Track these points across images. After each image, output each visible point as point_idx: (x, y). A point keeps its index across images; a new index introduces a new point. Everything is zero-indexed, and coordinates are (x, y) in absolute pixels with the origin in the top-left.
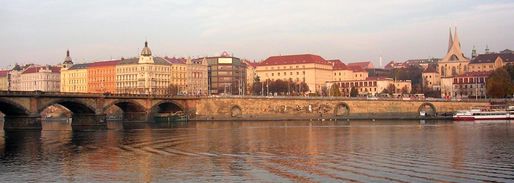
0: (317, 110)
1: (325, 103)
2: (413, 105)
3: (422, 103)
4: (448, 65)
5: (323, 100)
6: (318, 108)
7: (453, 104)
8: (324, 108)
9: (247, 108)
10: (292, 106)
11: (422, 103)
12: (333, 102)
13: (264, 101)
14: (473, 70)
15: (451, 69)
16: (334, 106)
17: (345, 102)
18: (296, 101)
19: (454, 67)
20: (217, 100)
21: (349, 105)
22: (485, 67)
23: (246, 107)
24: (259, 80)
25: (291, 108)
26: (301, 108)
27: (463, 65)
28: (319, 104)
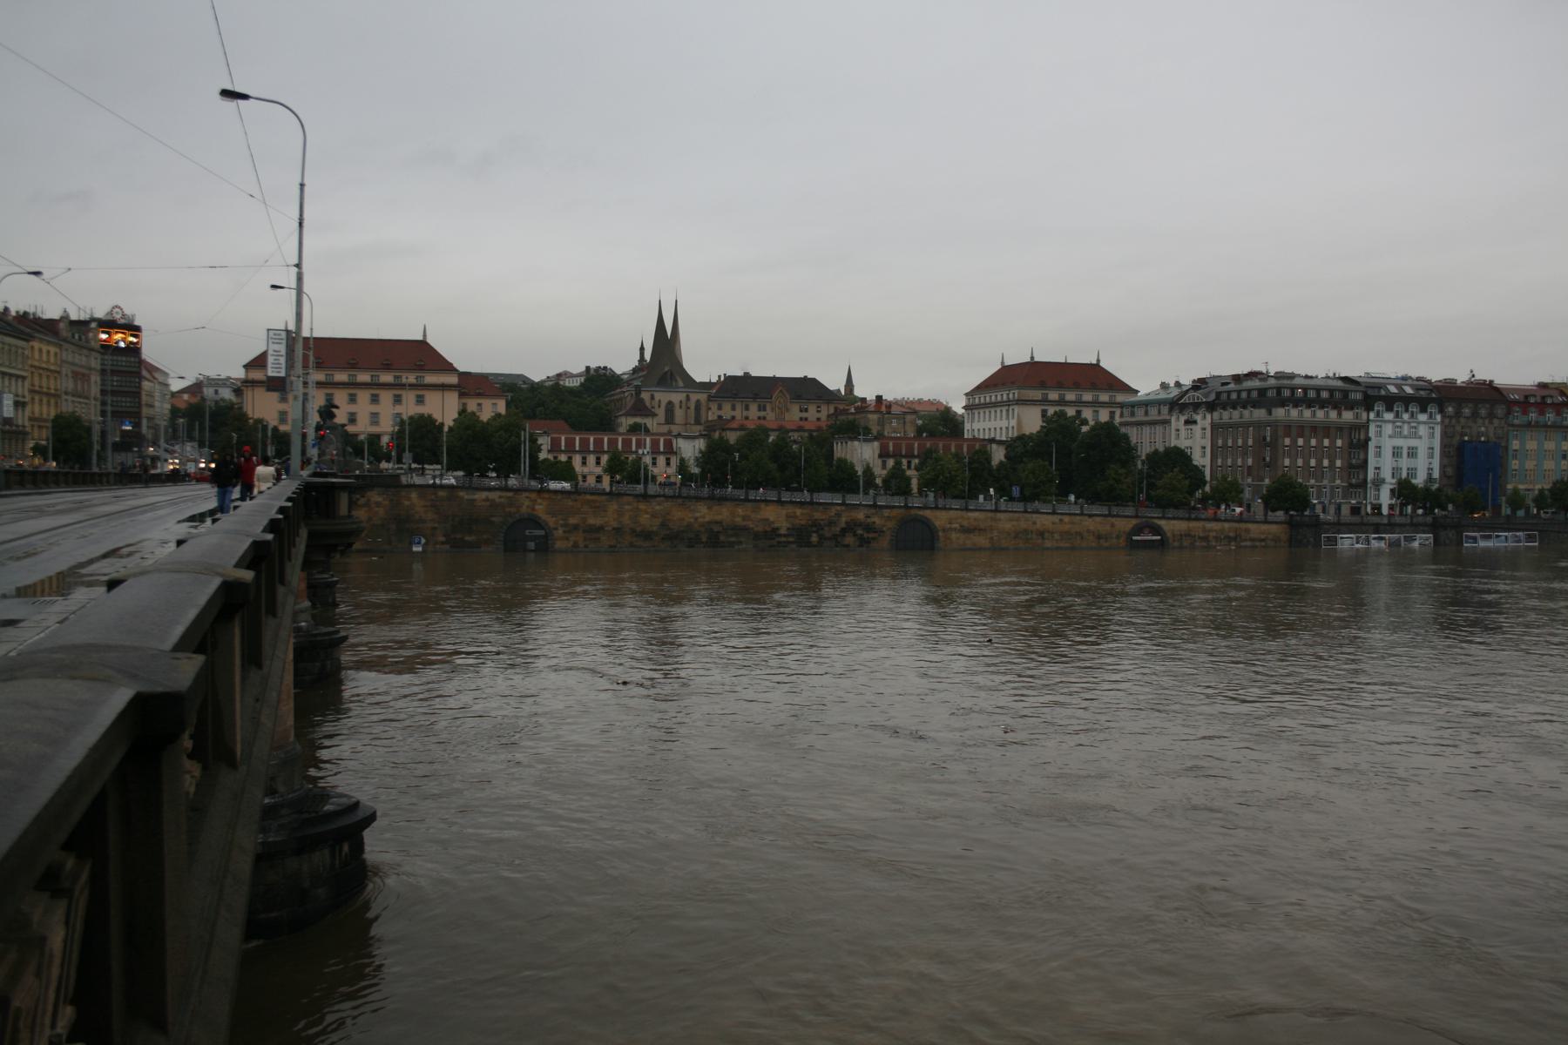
0: (835, 537)
2: (1113, 525)
3: (1134, 521)
4: (658, 396)
7: (1209, 525)
8: (860, 532)
9: (576, 527)
11: (1134, 521)
12: (886, 513)
13: (642, 506)
15: (663, 405)
16: (890, 524)
17: (927, 513)
18: (763, 505)
19: (670, 403)
20: (441, 493)
21: (937, 523)
22: (747, 408)
23: (572, 521)
24: (333, 416)
25: (745, 529)
26: (783, 531)
27: (694, 397)
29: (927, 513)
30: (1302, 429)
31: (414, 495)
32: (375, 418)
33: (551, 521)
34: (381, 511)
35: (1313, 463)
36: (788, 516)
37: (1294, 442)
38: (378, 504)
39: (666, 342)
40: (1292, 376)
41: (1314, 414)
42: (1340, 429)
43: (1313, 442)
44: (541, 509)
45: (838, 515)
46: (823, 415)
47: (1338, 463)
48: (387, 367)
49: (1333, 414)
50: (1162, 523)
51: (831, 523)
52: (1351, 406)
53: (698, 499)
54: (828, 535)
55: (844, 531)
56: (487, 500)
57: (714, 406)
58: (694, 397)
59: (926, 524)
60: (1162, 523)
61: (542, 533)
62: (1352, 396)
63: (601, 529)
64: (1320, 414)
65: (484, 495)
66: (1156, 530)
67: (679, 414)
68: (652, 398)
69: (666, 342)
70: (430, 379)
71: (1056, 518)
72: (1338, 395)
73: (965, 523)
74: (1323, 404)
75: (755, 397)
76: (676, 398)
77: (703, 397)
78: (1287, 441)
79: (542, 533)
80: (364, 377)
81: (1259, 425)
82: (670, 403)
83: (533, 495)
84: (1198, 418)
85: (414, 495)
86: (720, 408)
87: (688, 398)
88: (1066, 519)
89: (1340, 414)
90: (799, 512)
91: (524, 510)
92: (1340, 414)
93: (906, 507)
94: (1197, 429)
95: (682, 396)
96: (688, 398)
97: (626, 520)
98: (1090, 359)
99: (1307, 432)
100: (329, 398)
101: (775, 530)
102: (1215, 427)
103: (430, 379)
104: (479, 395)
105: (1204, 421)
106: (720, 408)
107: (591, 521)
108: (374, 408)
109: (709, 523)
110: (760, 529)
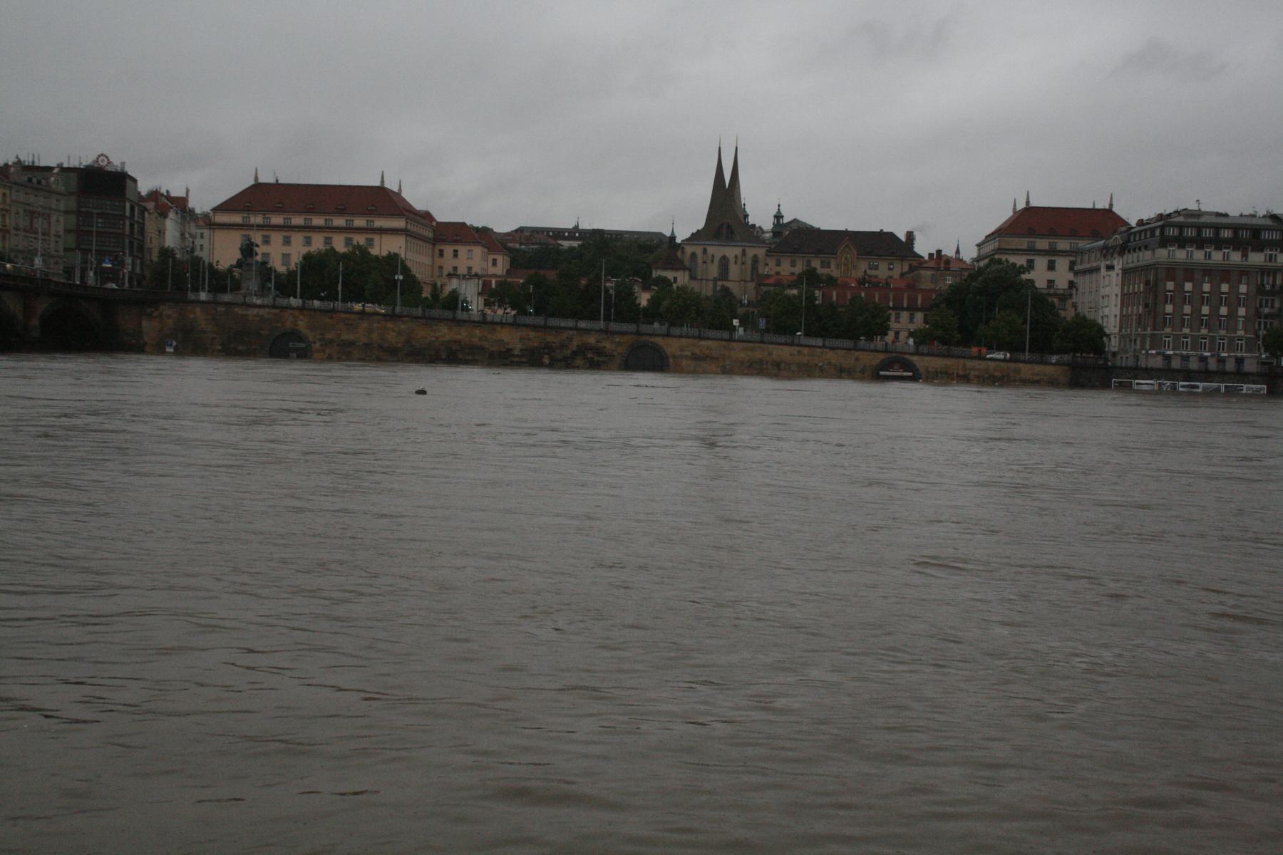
1: (592, 340)
3: (882, 356)
4: (710, 250)
5: (588, 331)
6: (568, 352)
7: (970, 363)
8: (590, 355)
9: (331, 341)
10: (486, 345)
11: (882, 356)
13: (390, 325)
14: (778, 269)
15: (716, 261)
17: (659, 340)
18: (498, 328)
19: (724, 258)
20: (221, 309)
21: (669, 351)
23: (330, 336)
25: (482, 348)
26: (516, 352)
27: (751, 252)
28: (575, 343)
29: (659, 340)
30: (1189, 272)
31: (198, 310)
32: (286, 257)
33: (310, 336)
34: (170, 322)
35: (1205, 310)
36: (521, 338)
37: (1180, 287)
38: (169, 317)
39: (725, 195)
40: (1198, 214)
41: (1226, 257)
42: (1244, 272)
43: (1206, 287)
44: (302, 324)
45: (570, 339)
46: (896, 273)
47: (1242, 311)
48: (341, 212)
49: (1236, 257)
50: (915, 359)
51: (563, 346)
52: (1259, 248)
53: (440, 320)
54: (560, 357)
55: (575, 354)
56: (257, 315)
57: (772, 262)
58: (751, 252)
59: (657, 349)
60: (915, 359)
61: (303, 345)
62: (1265, 235)
63: (351, 344)
64: (1217, 256)
65: (255, 311)
66: (907, 366)
67: (734, 270)
68: (705, 251)
69: (725, 195)
70: (380, 223)
71: (794, 349)
72: (1245, 234)
73: (697, 351)
74: (1219, 244)
75: (818, 252)
76: (732, 252)
77: (761, 252)
78: (1170, 285)
79: (303, 345)
80: (318, 221)
81: (1146, 268)
82: (724, 258)
83: (297, 313)
84: (1115, 262)
85: (198, 310)
86: (778, 264)
87: (744, 253)
88: (805, 351)
89: (1245, 256)
90: (532, 334)
91: (288, 325)
92: (1245, 256)
93: (638, 333)
94: (1113, 273)
95: (738, 251)
96: (744, 253)
97: (375, 336)
98: (1102, 204)
99: (1198, 276)
100: (248, 238)
101: (509, 350)
102: (1125, 271)
103: (380, 223)
104: (456, 242)
105: (1118, 264)
106: (778, 264)
107: (345, 337)
108: (286, 250)
109: (449, 342)
110: (495, 349)
